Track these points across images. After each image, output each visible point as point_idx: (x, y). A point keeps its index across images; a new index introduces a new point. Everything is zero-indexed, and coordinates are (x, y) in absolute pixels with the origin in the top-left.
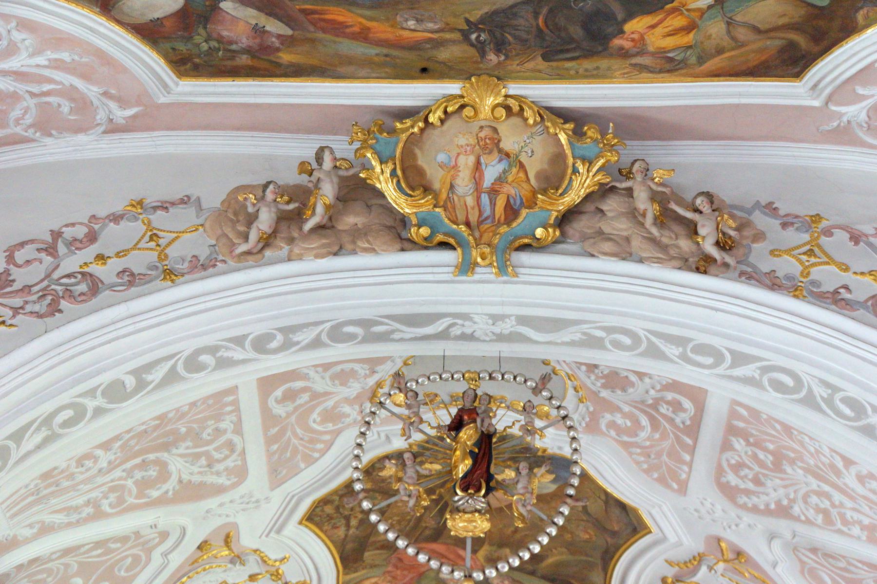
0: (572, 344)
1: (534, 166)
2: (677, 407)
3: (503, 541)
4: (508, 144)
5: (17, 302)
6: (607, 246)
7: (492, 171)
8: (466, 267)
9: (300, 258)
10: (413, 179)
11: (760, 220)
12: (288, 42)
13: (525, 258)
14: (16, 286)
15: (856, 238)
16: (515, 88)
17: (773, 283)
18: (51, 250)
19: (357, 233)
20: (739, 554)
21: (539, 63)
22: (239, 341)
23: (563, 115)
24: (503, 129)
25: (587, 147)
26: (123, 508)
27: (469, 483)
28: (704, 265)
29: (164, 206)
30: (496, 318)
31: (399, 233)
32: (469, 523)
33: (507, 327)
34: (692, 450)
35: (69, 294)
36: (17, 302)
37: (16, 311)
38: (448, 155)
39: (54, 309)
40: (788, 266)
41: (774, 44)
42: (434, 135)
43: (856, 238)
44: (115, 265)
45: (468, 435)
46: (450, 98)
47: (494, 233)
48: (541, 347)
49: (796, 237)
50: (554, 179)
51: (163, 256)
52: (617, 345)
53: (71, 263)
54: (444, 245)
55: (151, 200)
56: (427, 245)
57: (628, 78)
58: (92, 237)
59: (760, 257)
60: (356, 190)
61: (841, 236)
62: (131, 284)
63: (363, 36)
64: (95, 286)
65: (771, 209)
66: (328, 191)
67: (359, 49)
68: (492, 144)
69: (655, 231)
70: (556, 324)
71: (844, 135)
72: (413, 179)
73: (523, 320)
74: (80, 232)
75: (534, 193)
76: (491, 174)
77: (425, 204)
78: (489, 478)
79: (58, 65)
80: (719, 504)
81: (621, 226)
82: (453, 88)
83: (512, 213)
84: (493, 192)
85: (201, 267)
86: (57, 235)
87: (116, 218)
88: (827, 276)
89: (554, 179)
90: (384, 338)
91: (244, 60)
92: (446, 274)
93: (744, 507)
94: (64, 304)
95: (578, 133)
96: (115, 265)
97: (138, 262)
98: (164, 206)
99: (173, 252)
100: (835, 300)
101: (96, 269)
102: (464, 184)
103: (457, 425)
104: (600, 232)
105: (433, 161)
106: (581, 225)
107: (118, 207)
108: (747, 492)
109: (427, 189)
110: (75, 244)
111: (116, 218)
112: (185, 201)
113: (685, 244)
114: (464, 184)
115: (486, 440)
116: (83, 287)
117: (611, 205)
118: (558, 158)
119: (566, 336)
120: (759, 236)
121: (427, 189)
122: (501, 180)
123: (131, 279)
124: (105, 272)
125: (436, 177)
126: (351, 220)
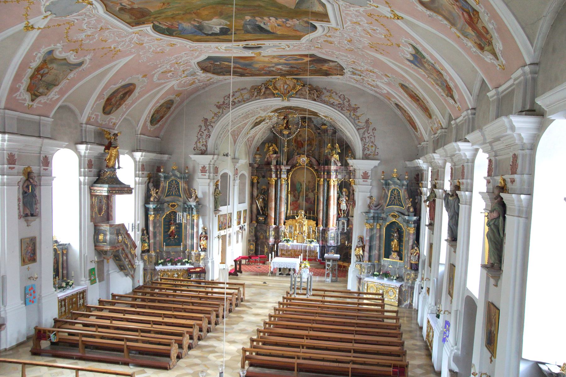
1: (292, 86)
3: (288, 136)
4: (288, 83)
7: (286, 87)
8: (283, 100)
11: (324, 91)
15: (336, 94)
17: (324, 102)
19: (269, 94)
25: (299, 83)
26: (244, 121)
27: (285, 128)
28: (315, 100)
29: (242, 89)
31: (274, 95)
32: (286, 132)
38: (280, 84)
40: (327, 99)
42: (277, 82)
47: (286, 95)
49: (328, 94)
50: (294, 88)
56: (278, 97)
59: (323, 98)
61: (334, 93)
65: (325, 89)
66: (263, 90)
68: (286, 83)
72: (276, 89)
77: (277, 91)
78: (288, 127)
83: (289, 92)
85: (248, 100)
87: (236, 92)
88: (332, 101)
89: (294, 88)
97: (240, 99)
98: (242, 89)
100: (332, 105)
102: (282, 88)
103: (284, 119)
105: (278, 85)
106: (299, 92)
107: (237, 90)
111: (236, 92)
112: (245, 89)
114: (282, 88)
115: (287, 122)
118: (295, 85)
120: (323, 94)
123: (239, 102)
124: (236, 101)
125: (278, 88)
126: (267, 92)
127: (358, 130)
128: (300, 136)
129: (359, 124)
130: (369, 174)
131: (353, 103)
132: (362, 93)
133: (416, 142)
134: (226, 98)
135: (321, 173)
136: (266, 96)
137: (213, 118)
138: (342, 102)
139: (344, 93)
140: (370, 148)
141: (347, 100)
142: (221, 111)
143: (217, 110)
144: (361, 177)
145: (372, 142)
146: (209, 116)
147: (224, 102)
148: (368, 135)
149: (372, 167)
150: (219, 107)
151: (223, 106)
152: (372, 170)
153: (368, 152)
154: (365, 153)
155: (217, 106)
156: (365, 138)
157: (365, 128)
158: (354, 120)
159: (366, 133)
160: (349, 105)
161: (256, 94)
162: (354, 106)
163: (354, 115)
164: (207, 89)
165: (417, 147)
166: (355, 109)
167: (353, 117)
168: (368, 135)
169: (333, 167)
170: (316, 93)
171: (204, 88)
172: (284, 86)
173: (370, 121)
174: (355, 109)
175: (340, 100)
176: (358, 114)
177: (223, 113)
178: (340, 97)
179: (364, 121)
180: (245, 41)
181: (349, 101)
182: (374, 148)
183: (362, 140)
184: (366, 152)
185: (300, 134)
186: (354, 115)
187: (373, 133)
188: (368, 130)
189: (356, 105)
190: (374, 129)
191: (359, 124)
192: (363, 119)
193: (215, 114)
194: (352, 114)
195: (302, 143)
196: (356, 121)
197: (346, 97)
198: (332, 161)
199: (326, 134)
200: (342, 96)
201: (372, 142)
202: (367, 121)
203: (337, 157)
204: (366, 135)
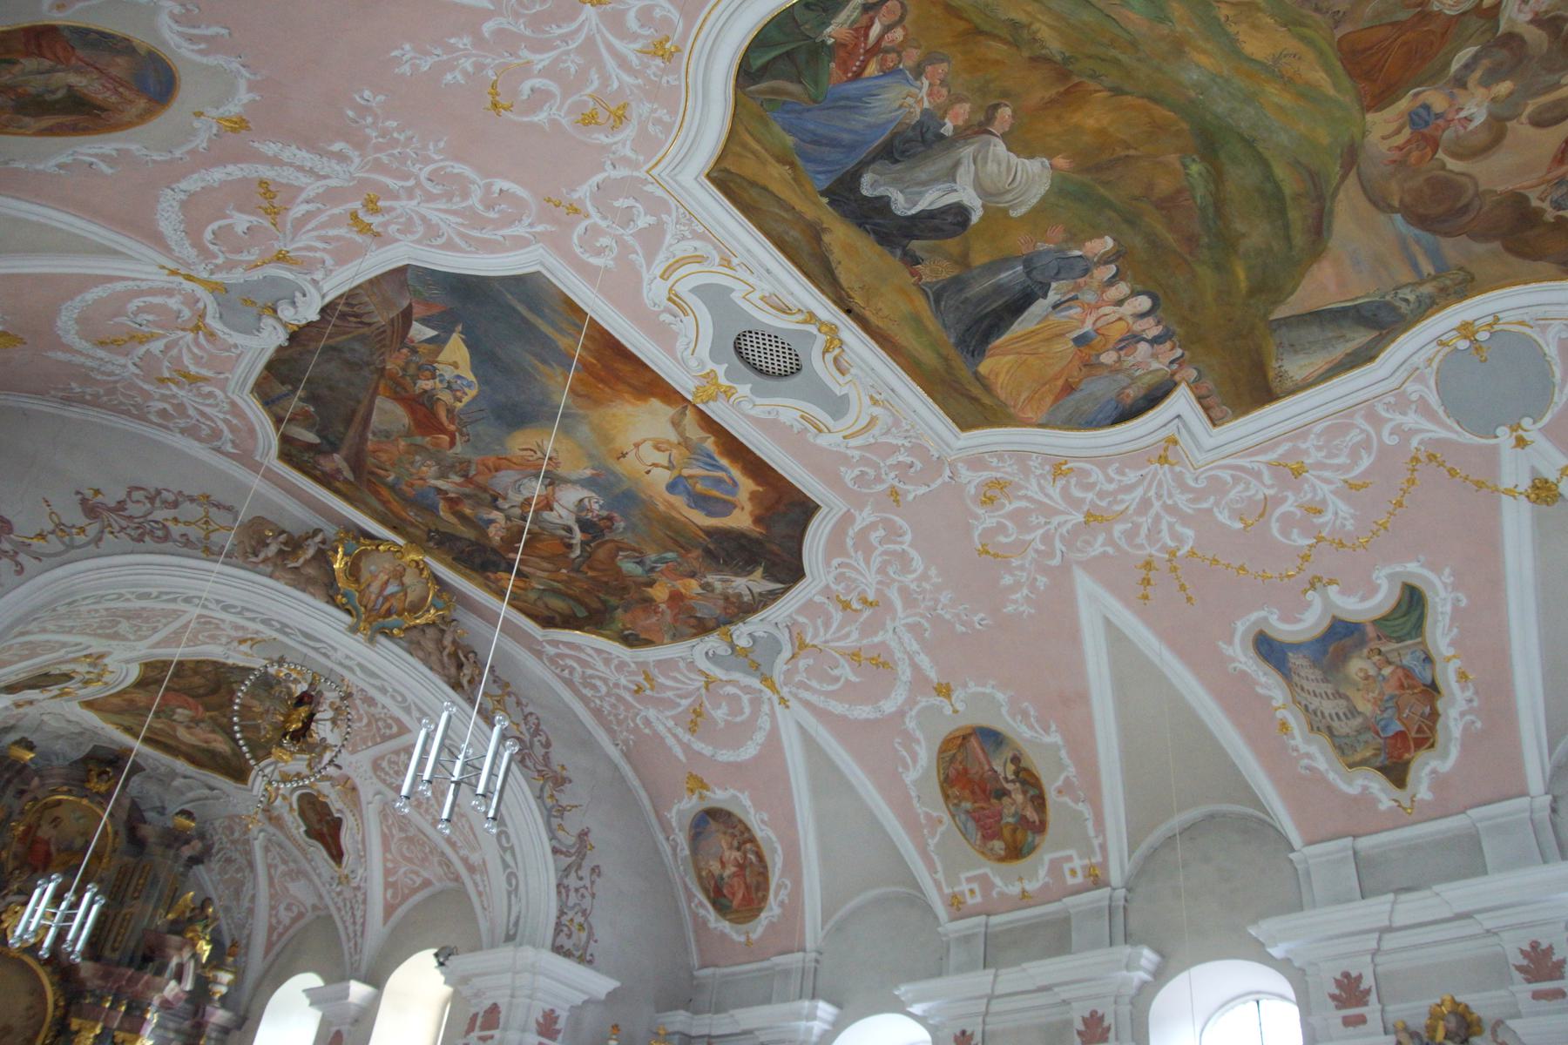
0: (373, 686)
1: (412, 596)
2: (390, 727)
4: (407, 580)
5: (124, 523)
6: (421, 654)
7: (391, 589)
8: (354, 629)
9: (277, 579)
10: (353, 571)
12: (346, 480)
13: (382, 639)
14: (126, 513)
15: (519, 703)
16: (428, 559)
18: (152, 499)
20: (354, 789)
21: (449, 559)
22: (218, 602)
23: (438, 580)
24: (409, 572)
29: (218, 506)
30: (347, 657)
31: (331, 593)
33: (347, 662)
34: (376, 744)
35: (151, 532)
36: (124, 523)
37: (123, 529)
38: (377, 569)
39: (140, 539)
41: (546, 613)
43: (519, 703)
44: (181, 528)
45: (303, 711)
46: (395, 544)
47: (376, 619)
48: (356, 680)
51: (207, 538)
52: (393, 697)
53: (160, 514)
54: (349, 612)
55: (215, 497)
57: (479, 585)
58: (175, 505)
60: (323, 557)
61: (513, 699)
62: (185, 545)
63: (385, 503)
64: (166, 538)
67: (380, 508)
68: (399, 575)
69: (446, 659)
70: (373, 675)
71: (539, 654)
73: (359, 665)
74: (171, 498)
75: (404, 610)
76: (391, 589)
79: (225, 421)
80: (367, 767)
81: (430, 646)
82: (401, 541)
83: (389, 613)
84: (386, 599)
86: (158, 492)
87: (192, 499)
89: (415, 608)
90: (287, 634)
91: (318, 473)
92: (342, 627)
93: (379, 777)
94: (147, 538)
95: (438, 595)
96: (181, 528)
97: (195, 533)
98: (218, 506)
99: (214, 537)
101: (170, 524)
102: (375, 587)
104: (419, 643)
105: (368, 567)
107: (195, 493)
108: (387, 773)
109: (357, 581)
110: (167, 504)
111: (192, 499)
112: (229, 509)
113: (453, 671)
114: (375, 587)
116: (160, 533)
117: (431, 632)
119: (378, 683)
121: (357, 581)
122: (392, 595)
123: (187, 542)
124: (176, 530)
125: (365, 575)
127: (555, 851)
128: (56, 821)
129: (560, 834)
130: (561, 1024)
131: (559, 755)
132: (586, 743)
133: (695, 960)
134: (136, 495)
135: (102, 998)
136: (301, 581)
137: (41, 536)
138: (527, 737)
139: (539, 712)
140: (574, 928)
141: (543, 739)
142: (93, 529)
143: (76, 517)
144: (534, 1026)
145: (584, 912)
146: (26, 521)
147: (121, 506)
148: (581, 883)
149: (579, 998)
150: (91, 510)
151: (116, 521)
152: (574, 1009)
153: (568, 944)
154: (558, 943)
155: (84, 501)
156: (567, 888)
157: (573, 855)
158: (554, 813)
159: (573, 874)
160: (546, 757)
161: (273, 549)
162: (558, 769)
163: (552, 796)
164: (74, 412)
165: (692, 977)
166: (560, 781)
167: (549, 802)
168: (581, 883)
169: (171, 989)
170: (458, 666)
171: (68, 400)
172: (386, 583)
173: (592, 839)
174: (560, 781)
175: (523, 728)
176: (564, 800)
177: (98, 540)
178: (525, 718)
179: (575, 831)
180: (848, 312)
181: (548, 745)
182: (584, 935)
183: (559, 893)
184: (562, 940)
185: (57, 812)
186: (552, 796)
187: (593, 883)
188: (579, 867)
189: (563, 767)
190: (595, 870)
191: (560, 834)
192: (572, 824)
193: (60, 528)
194: (547, 791)
195: (48, 854)
196: (555, 822)
197: (542, 727)
198: (174, 961)
199: (172, 853)
200: (532, 719)
201: (584, 912)
202: (583, 835)
203: (205, 949)
204: (572, 881)
